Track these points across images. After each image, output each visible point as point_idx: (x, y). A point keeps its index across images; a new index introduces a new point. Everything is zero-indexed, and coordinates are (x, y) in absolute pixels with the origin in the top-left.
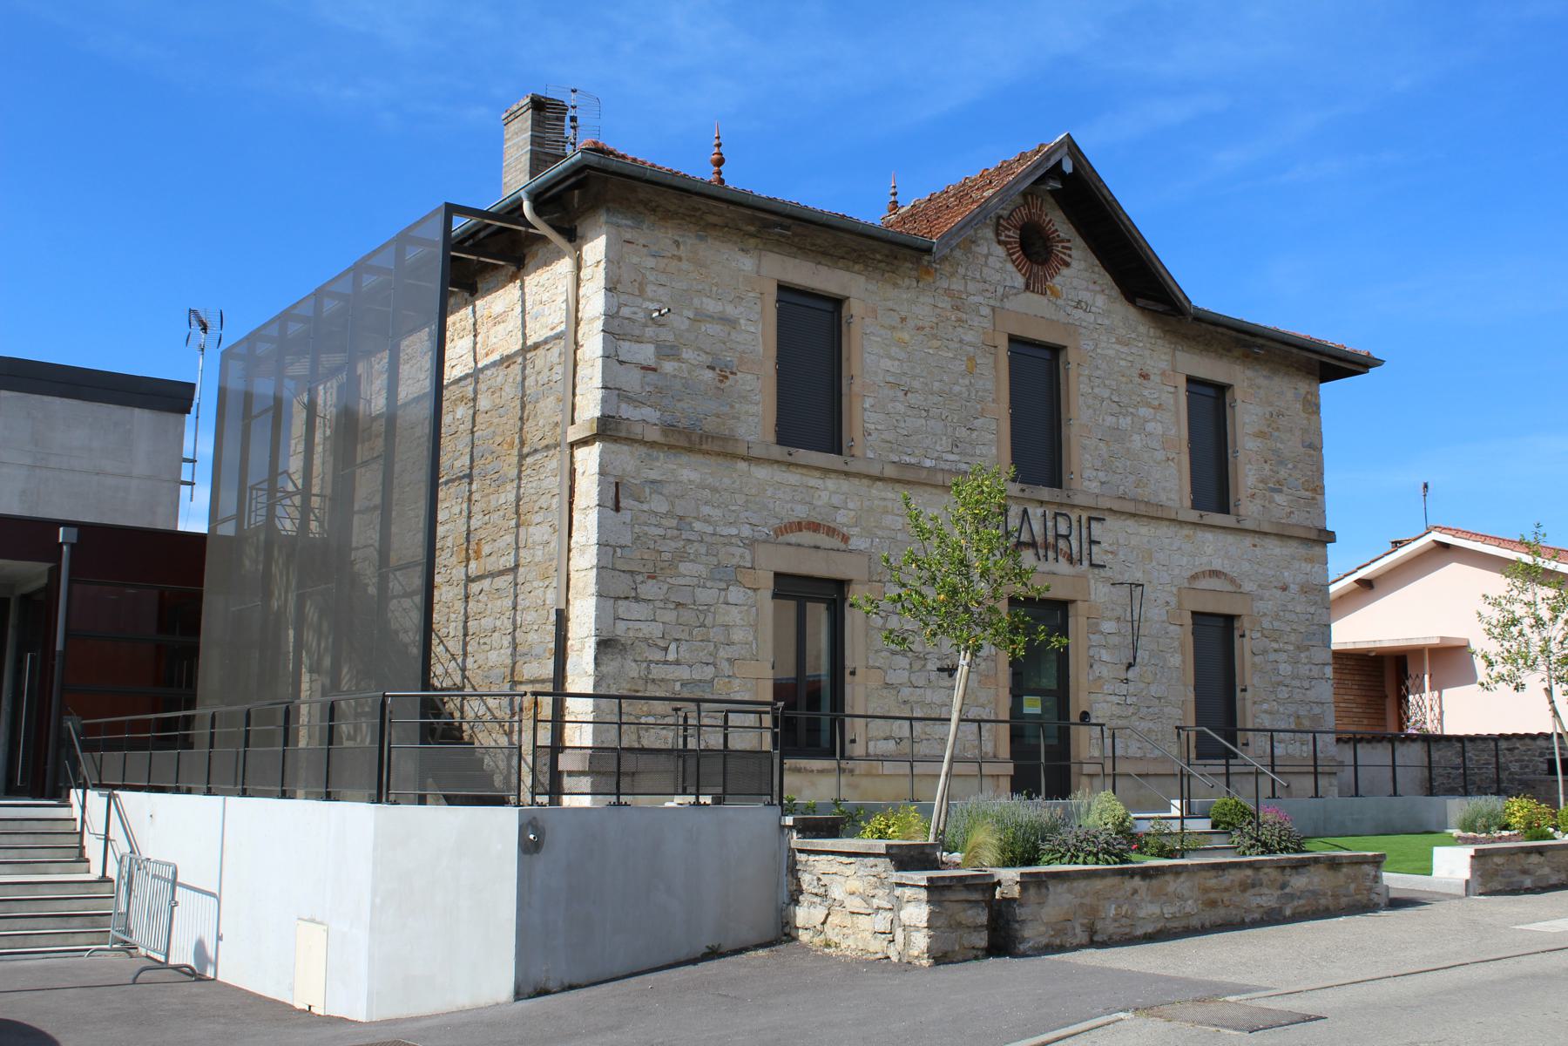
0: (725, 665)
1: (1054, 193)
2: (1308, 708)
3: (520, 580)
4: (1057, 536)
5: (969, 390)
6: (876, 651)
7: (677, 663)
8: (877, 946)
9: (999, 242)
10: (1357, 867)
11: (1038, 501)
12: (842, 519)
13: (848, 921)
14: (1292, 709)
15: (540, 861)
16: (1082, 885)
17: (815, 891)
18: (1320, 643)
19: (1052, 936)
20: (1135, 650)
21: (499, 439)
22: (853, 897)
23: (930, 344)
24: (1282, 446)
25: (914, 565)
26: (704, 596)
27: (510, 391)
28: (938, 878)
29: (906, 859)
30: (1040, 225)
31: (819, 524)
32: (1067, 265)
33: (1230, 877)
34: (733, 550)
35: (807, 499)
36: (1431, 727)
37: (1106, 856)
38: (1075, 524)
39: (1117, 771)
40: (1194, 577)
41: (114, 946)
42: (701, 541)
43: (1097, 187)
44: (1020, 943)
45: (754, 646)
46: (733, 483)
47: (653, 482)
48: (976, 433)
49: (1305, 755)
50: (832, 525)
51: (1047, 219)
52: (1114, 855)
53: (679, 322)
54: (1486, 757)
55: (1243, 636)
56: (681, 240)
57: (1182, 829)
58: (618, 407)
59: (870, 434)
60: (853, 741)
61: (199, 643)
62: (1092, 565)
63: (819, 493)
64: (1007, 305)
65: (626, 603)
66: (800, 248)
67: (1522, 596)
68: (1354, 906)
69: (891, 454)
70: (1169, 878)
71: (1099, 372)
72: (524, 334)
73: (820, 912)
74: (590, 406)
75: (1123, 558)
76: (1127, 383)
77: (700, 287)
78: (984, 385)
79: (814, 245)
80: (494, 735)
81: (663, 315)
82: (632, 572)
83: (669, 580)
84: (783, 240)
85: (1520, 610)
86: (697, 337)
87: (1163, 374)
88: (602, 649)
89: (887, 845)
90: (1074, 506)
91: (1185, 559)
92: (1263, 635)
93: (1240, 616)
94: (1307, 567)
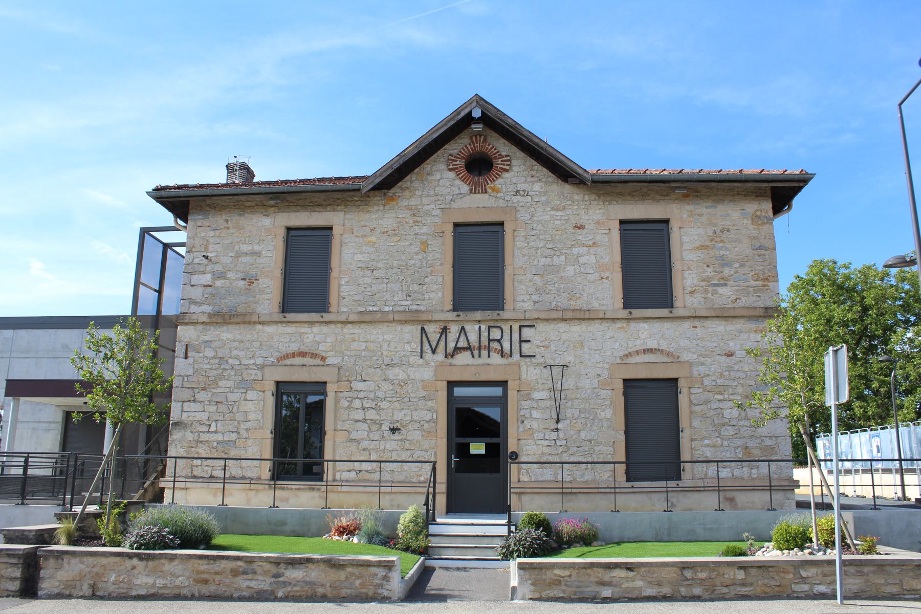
2: (759, 441)
6: (343, 421)
7: (216, 432)
9: (450, 170)
11: (476, 321)
12: (322, 347)
14: (739, 442)
24: (727, 253)
26: (232, 397)
30: (471, 154)
31: (306, 353)
33: (222, 566)
34: (250, 371)
45: (262, 421)
48: (426, 286)
49: (755, 476)
50: (315, 352)
58: (189, 308)
59: (344, 298)
62: (521, 356)
63: (308, 335)
64: (454, 205)
65: (188, 403)
66: (302, 206)
68: (357, 596)
69: (358, 308)
75: (555, 349)
76: (561, 235)
78: (434, 256)
79: (312, 202)
82: (193, 388)
90: (507, 320)
91: (618, 344)
92: (704, 391)
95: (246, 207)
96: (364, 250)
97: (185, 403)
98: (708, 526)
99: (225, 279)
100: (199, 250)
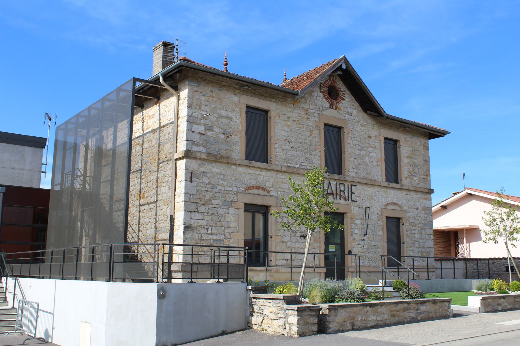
0: (228, 235)
1: (339, 75)
3: (158, 206)
4: (340, 191)
5: (310, 142)
6: (279, 230)
7: (212, 234)
8: (280, 330)
9: (321, 92)
10: (442, 303)
11: (334, 179)
12: (267, 185)
13: (270, 322)
14: (420, 249)
15: (165, 301)
16: (349, 309)
17: (258, 312)
18: (429, 227)
19: (340, 327)
20: (367, 229)
21: (151, 158)
22: (271, 314)
23: (297, 126)
24: (416, 161)
25: (292, 201)
26: (221, 211)
27: (155, 141)
28: (300, 307)
29: (290, 301)
30: (335, 86)
32: (344, 100)
33: (400, 307)
34: (231, 195)
35: (256, 178)
36: (466, 256)
37: (357, 300)
38: (346, 187)
39: (361, 271)
40: (387, 205)
41: (17, 331)
42: (220, 193)
43: (353, 73)
44: (328, 329)
45: (238, 228)
46: (231, 173)
47: (204, 172)
48: (313, 156)
49: (424, 265)
51: (337, 84)
52: (360, 299)
53: (213, 118)
54: (485, 266)
55: (403, 225)
56: (213, 90)
57: (383, 290)
59: (277, 156)
60: (271, 260)
61: (47, 227)
62: (352, 201)
64: (324, 113)
66: (254, 94)
67: (497, 211)
68: (441, 316)
69: (284, 163)
70: (379, 307)
71: (354, 136)
72: (160, 122)
73: (260, 319)
74: (182, 147)
76: (364, 140)
77: (220, 107)
79: (258, 92)
80: (149, 258)
81: (207, 116)
82: (196, 203)
83: (209, 206)
84: (248, 91)
85: (496, 216)
86: (219, 124)
87: (376, 136)
88: (186, 229)
89: (283, 296)
90: (346, 181)
91: (383, 199)
92: (410, 225)
93: (402, 218)
94: (425, 202)
95: (223, 85)
96: (285, 129)
97: (192, 213)
98: (441, 286)
99: (213, 131)
100: (196, 107)
